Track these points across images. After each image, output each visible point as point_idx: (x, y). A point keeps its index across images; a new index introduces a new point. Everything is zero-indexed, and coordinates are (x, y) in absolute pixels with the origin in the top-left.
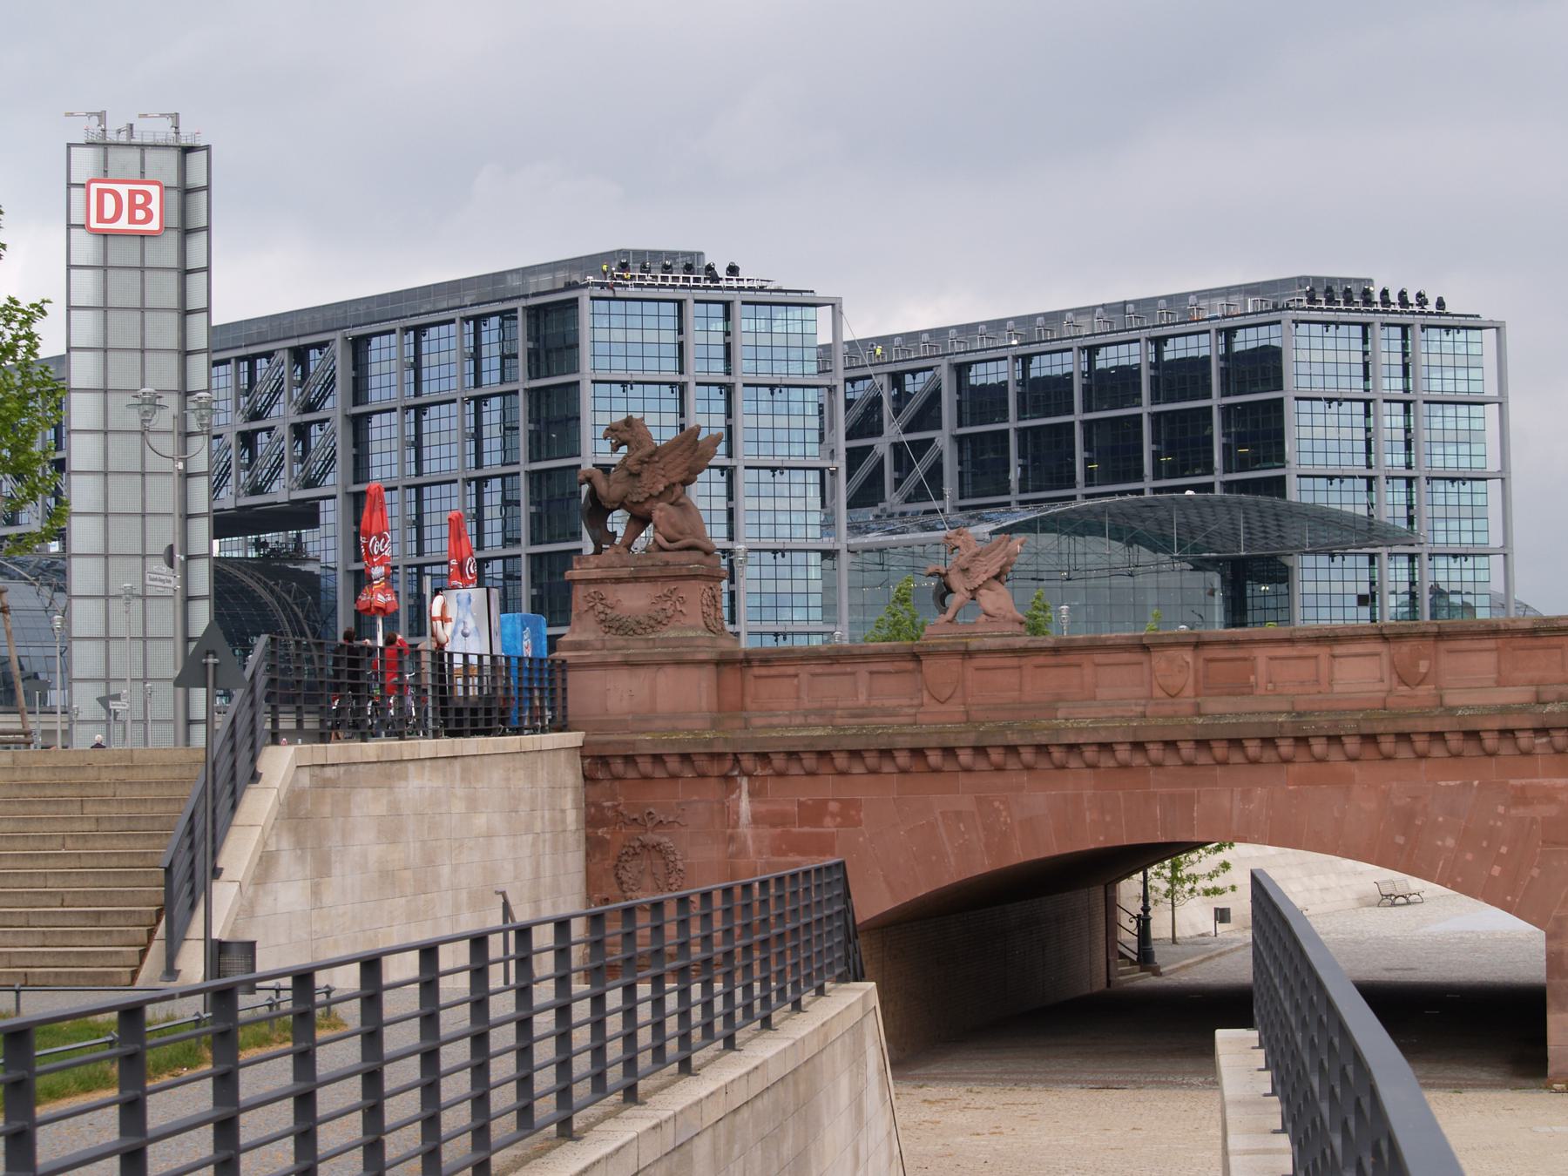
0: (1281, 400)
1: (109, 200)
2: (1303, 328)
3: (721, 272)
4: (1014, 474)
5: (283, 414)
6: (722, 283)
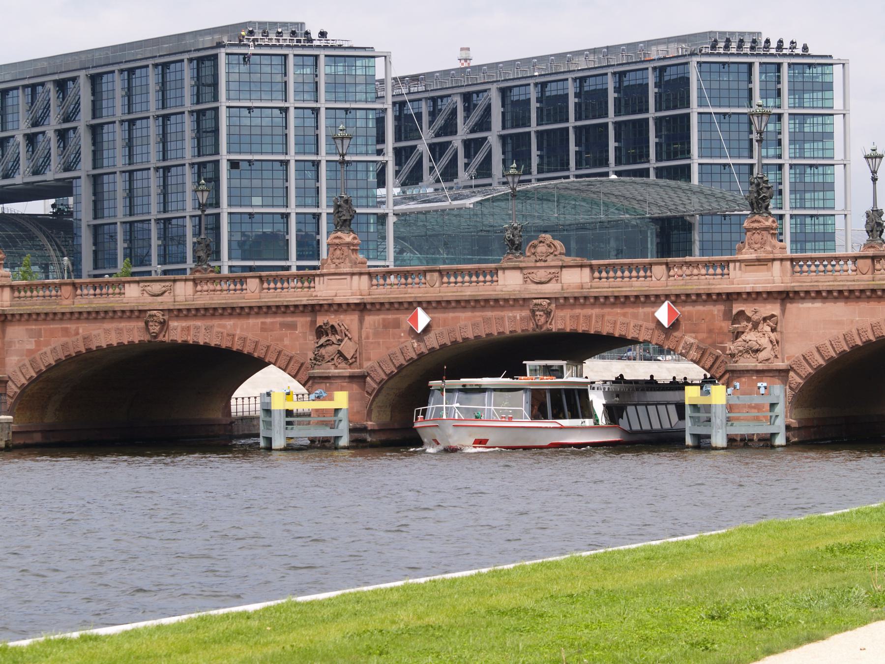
0: (689, 114)
2: (705, 67)
3: (315, 35)
4: (535, 161)
5: (53, 123)
6: (316, 43)
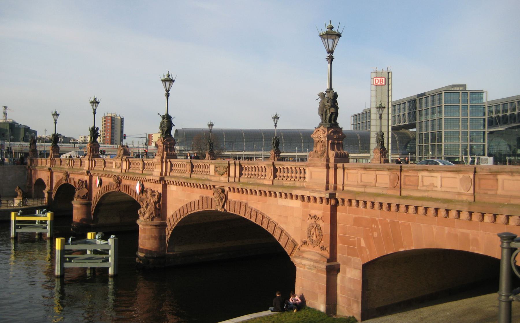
1: (377, 81)
